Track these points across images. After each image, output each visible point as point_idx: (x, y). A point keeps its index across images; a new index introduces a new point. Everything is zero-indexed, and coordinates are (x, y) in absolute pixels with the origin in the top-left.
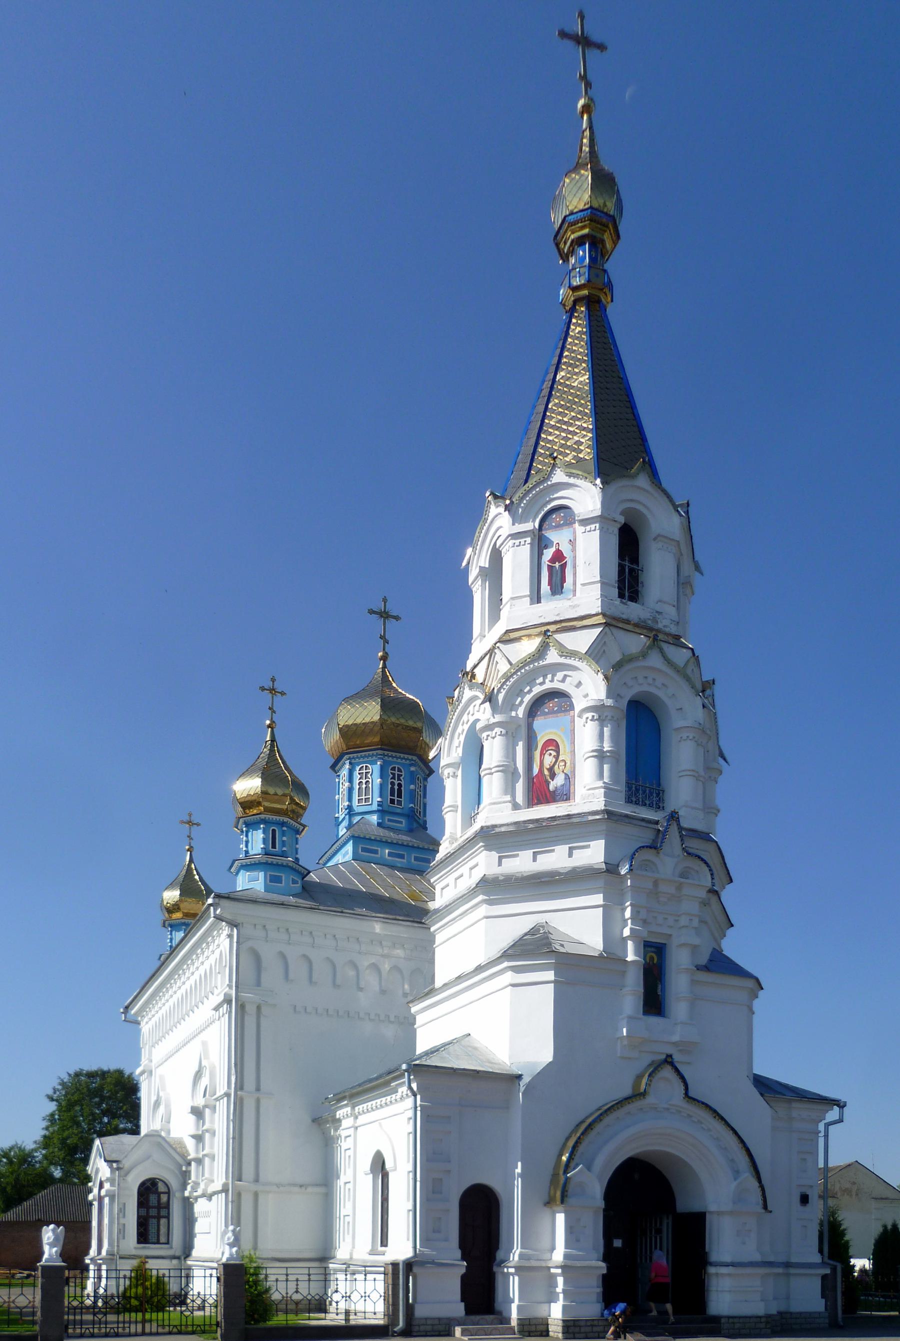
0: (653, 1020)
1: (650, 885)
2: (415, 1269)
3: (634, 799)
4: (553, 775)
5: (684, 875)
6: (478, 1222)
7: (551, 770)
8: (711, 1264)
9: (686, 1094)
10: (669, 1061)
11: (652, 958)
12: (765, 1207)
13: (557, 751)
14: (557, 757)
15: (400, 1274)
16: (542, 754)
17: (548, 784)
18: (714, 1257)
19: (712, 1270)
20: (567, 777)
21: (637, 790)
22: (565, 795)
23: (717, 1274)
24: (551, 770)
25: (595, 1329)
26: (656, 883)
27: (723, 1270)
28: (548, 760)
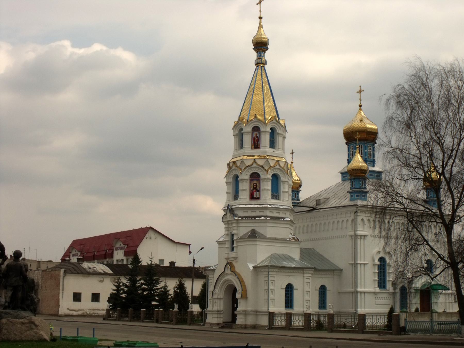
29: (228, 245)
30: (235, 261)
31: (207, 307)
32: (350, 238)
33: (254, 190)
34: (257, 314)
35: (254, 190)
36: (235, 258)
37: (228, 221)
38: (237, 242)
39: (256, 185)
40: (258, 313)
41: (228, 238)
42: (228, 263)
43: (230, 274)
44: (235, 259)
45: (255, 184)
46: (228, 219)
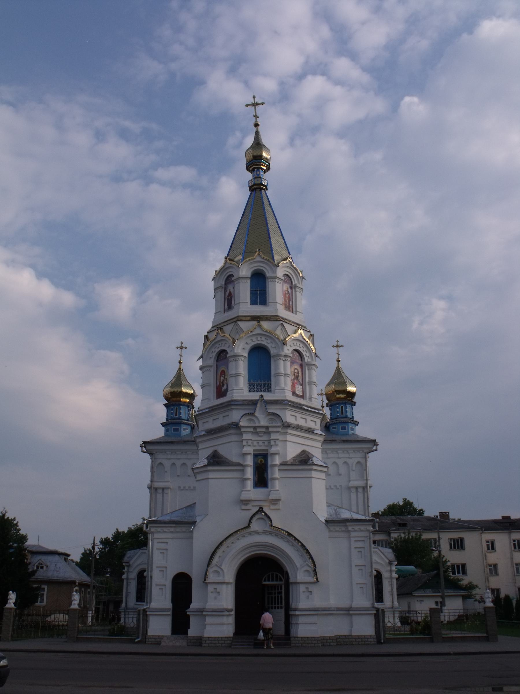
1: (252, 430)
3: (256, 390)
4: (223, 385)
10: (261, 510)
11: (261, 461)
13: (225, 375)
14: (224, 377)
16: (220, 377)
17: (222, 389)
21: (257, 385)
24: (223, 383)
25: (220, 642)
28: (222, 378)
29: (250, 473)
30: (273, 507)
31: (151, 602)
32: (354, 490)
33: (295, 381)
34: (351, 615)
35: (295, 381)
36: (275, 502)
37: (255, 428)
38: (279, 470)
39: (298, 373)
40: (351, 612)
41: (249, 461)
42: (261, 510)
43: (265, 532)
44: (275, 504)
45: (296, 371)
46: (257, 424)
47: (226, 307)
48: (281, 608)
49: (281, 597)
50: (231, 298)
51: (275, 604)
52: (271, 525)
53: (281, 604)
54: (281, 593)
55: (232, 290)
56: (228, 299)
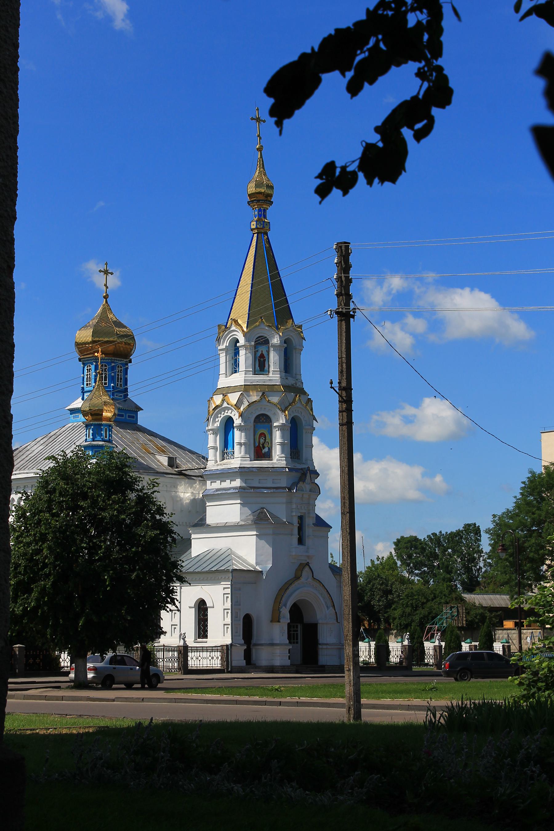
0: (301, 547)
2: (233, 647)
4: (264, 447)
5: (310, 491)
6: (245, 627)
7: (263, 445)
8: (320, 644)
9: (313, 576)
10: (308, 564)
12: (337, 621)
13: (265, 437)
14: (265, 440)
15: (226, 651)
16: (259, 438)
18: (321, 641)
19: (320, 647)
20: (269, 448)
22: (268, 456)
23: (322, 648)
24: (263, 445)
26: (303, 495)
27: (325, 647)
47: (257, 368)
48: (297, 643)
49: (297, 634)
50: (264, 361)
51: (294, 640)
52: (313, 576)
53: (297, 639)
54: (297, 631)
55: (265, 353)
56: (259, 360)
